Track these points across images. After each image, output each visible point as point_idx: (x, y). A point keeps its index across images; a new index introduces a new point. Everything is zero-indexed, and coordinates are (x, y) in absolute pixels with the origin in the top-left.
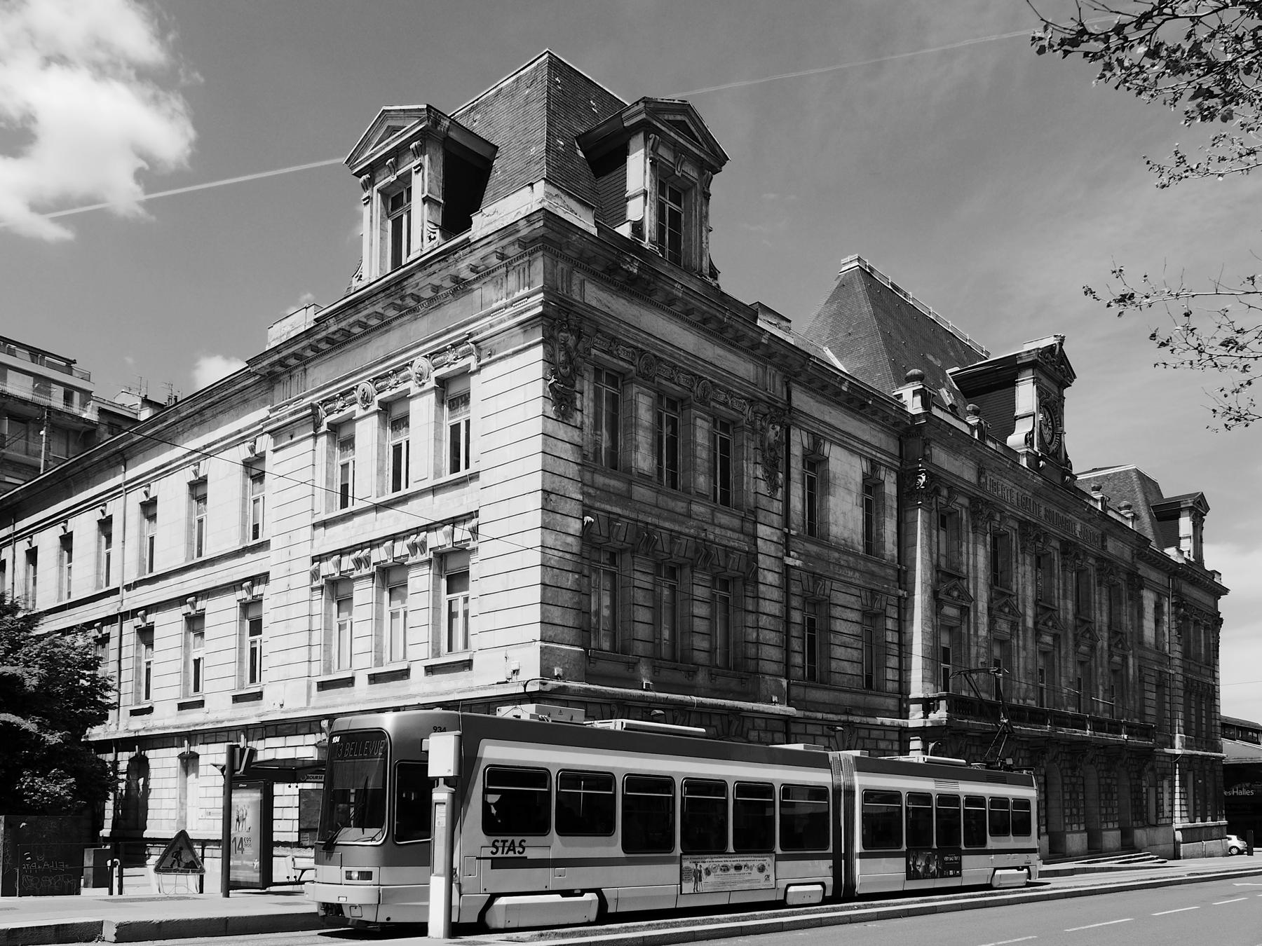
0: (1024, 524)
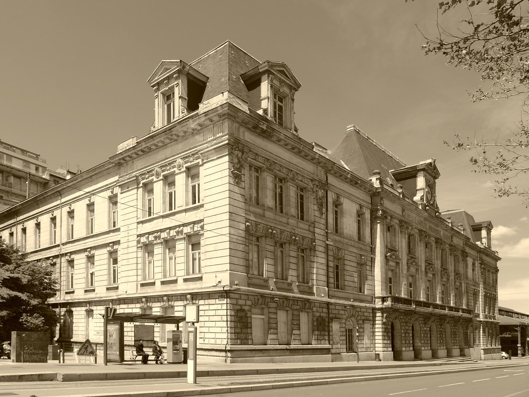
0: (420, 231)
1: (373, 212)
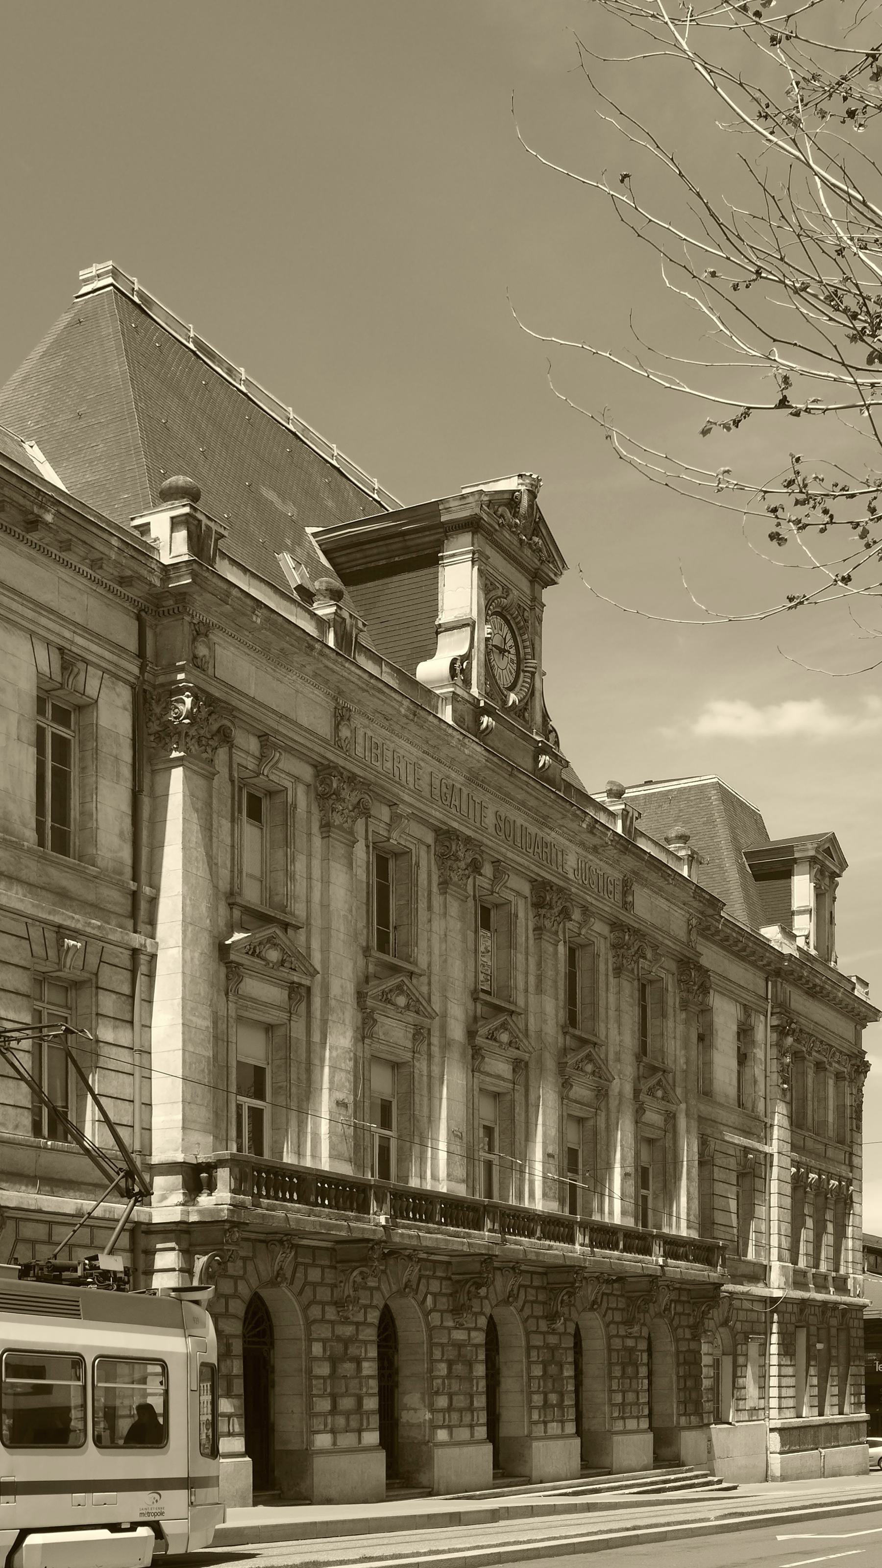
0: (445, 835)
1: (148, 702)
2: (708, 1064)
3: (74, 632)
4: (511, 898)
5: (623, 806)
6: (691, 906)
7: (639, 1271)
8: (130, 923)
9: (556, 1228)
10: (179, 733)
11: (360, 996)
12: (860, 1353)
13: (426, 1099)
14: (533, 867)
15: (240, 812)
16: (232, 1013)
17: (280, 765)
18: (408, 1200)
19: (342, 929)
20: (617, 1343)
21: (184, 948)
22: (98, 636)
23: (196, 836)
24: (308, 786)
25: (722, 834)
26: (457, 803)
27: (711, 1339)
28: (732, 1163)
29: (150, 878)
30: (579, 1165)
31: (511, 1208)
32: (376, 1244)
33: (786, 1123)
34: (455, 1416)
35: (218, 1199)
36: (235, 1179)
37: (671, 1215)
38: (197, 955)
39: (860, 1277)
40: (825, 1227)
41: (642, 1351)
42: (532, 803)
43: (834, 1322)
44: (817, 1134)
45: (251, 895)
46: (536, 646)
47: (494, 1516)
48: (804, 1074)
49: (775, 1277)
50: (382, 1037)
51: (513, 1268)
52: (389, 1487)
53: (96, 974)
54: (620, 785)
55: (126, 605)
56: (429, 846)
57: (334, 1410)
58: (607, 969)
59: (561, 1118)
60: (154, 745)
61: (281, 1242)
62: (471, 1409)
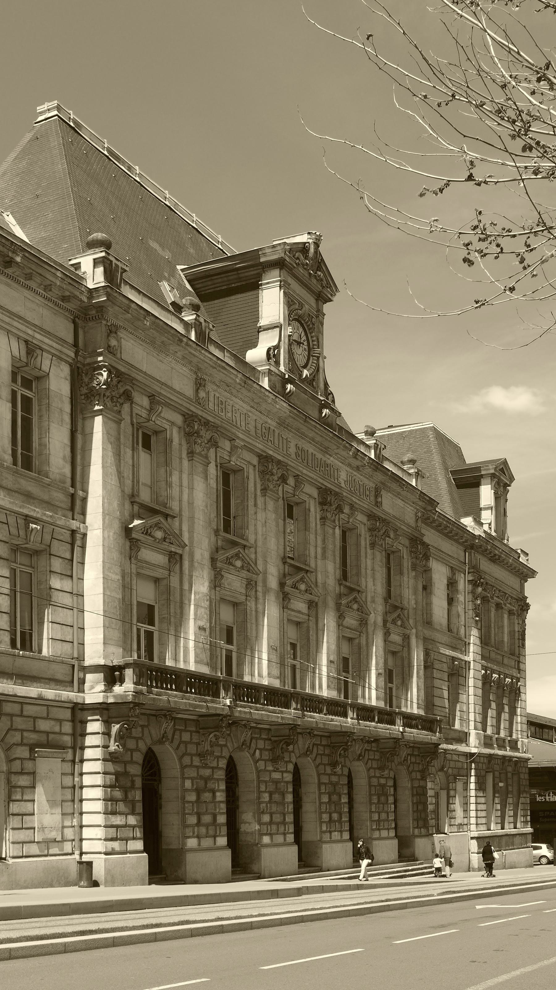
0: (264, 459)
1: (80, 375)
2: (429, 604)
3: (34, 331)
4: (306, 499)
5: (375, 441)
6: (417, 505)
7: (388, 735)
8: (70, 514)
9: (336, 708)
10: (100, 394)
11: (213, 560)
12: (526, 789)
13: (254, 626)
14: (320, 480)
15: (138, 444)
16: (134, 571)
17: (162, 415)
18: (244, 690)
19: (201, 518)
20: (374, 781)
21: (103, 530)
22: (49, 333)
23: (111, 459)
24: (180, 428)
25: (437, 459)
26: (272, 439)
27: (433, 779)
28: (445, 667)
29: (83, 486)
30: (350, 667)
31: (307, 695)
32: (225, 717)
33: (478, 642)
34: (274, 827)
35: (126, 688)
36: (136, 675)
37: (407, 700)
38: (111, 534)
39: (526, 741)
40: (503, 708)
41: (390, 787)
42: (318, 439)
43: (510, 769)
44: (498, 649)
45: (145, 496)
46: (320, 340)
47: (299, 892)
48: (489, 611)
49: (473, 740)
50: (227, 586)
51: (309, 733)
52: (233, 873)
53: (50, 546)
54: (372, 428)
55: (66, 314)
56: (254, 466)
57: (199, 823)
58: (366, 544)
59: (338, 638)
60: (84, 401)
61: (165, 716)
62: (284, 823)
